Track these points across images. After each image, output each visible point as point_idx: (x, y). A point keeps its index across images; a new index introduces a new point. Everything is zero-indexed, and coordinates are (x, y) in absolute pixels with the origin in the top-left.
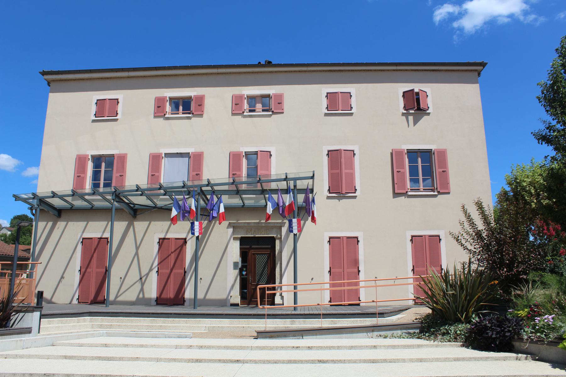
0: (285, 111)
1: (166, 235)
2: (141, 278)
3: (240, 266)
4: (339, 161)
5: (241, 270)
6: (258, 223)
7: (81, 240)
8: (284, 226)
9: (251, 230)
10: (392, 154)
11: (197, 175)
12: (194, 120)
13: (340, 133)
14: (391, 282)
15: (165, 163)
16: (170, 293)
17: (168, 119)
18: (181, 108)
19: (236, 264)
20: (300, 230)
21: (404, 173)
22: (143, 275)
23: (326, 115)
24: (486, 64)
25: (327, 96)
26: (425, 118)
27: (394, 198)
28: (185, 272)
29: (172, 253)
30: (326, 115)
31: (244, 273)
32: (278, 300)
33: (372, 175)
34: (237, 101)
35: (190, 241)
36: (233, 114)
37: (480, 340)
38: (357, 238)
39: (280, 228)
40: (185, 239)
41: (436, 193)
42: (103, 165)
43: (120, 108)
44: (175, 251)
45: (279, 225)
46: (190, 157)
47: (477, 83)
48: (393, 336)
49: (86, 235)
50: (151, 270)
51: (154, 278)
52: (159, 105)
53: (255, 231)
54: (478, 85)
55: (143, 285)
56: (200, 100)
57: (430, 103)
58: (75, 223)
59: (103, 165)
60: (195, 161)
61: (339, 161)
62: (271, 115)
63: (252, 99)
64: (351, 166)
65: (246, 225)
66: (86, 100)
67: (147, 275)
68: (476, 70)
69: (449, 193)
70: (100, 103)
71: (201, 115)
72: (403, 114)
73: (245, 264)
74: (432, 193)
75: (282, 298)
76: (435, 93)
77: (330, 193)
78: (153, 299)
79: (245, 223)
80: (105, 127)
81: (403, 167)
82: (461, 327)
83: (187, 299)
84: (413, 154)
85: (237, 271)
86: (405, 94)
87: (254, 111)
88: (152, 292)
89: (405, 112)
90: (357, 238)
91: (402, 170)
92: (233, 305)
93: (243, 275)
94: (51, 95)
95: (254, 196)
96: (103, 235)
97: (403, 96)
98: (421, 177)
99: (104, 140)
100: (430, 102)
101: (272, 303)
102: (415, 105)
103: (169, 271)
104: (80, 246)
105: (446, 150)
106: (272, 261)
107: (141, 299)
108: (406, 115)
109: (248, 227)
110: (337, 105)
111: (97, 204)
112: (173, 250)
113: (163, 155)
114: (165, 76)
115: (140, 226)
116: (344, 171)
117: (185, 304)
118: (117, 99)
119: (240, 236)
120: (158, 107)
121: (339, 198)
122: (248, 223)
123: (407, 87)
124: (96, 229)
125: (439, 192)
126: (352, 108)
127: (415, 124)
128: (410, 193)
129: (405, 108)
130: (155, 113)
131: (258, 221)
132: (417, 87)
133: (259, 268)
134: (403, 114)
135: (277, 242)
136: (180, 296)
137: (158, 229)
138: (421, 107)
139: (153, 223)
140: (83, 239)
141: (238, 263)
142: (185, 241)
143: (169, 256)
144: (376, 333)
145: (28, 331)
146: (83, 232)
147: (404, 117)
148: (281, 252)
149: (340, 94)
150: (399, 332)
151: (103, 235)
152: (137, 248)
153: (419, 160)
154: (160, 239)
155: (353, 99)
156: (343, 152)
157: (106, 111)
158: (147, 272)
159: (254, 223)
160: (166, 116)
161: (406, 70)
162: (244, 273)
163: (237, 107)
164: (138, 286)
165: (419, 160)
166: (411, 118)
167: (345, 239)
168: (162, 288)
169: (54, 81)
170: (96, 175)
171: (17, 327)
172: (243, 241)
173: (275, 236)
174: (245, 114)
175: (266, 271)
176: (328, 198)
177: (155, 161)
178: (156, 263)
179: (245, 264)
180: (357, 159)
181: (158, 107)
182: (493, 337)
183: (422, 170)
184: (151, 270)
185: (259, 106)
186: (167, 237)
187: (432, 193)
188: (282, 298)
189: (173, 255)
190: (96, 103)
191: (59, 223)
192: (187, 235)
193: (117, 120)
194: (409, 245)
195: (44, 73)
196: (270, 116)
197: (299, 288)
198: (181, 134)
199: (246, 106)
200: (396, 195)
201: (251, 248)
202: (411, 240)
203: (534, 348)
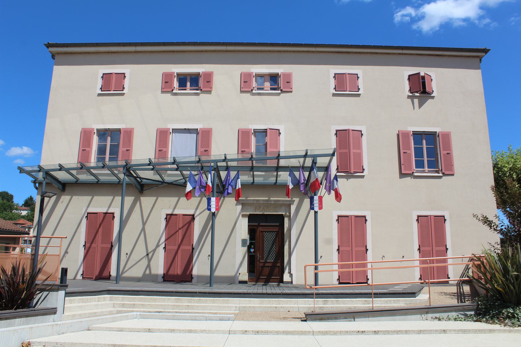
0: (293, 90)
2: (148, 255)
3: (248, 243)
5: (249, 248)
6: (267, 200)
7: (86, 215)
8: (293, 204)
9: (260, 207)
11: (205, 151)
12: (203, 96)
15: (173, 138)
16: (178, 270)
17: (176, 94)
18: (188, 84)
19: (244, 242)
20: (321, 208)
21: (410, 154)
22: (149, 251)
24: (489, 50)
25: (334, 77)
26: (430, 101)
27: (400, 178)
28: (193, 249)
29: (180, 229)
30: (334, 95)
31: (252, 250)
32: (286, 277)
33: (379, 155)
35: (198, 217)
36: (242, 92)
38: (365, 217)
39: (289, 206)
40: (193, 215)
41: (441, 175)
44: (182, 227)
45: (288, 203)
49: (91, 210)
50: (158, 246)
51: (161, 253)
52: (167, 79)
53: (263, 209)
54: (480, 70)
55: (149, 261)
56: (209, 77)
57: (434, 86)
58: (80, 197)
60: (203, 137)
62: (279, 94)
64: (359, 146)
65: (255, 202)
66: (93, 73)
67: (154, 251)
68: (478, 57)
69: (453, 175)
70: (106, 77)
71: (209, 92)
72: (409, 97)
73: (254, 241)
74: (437, 174)
75: (291, 275)
76: (439, 77)
78: (160, 275)
79: (254, 200)
80: (111, 102)
81: (409, 149)
83: (195, 276)
84: (418, 136)
85: (246, 248)
89: (411, 94)
90: (365, 217)
91: (408, 151)
92: (241, 282)
93: (250, 252)
94: (55, 67)
95: (263, 173)
96: (108, 210)
97: (409, 79)
98: (426, 159)
99: (110, 114)
100: (434, 85)
101: (281, 281)
102: (420, 88)
104: (84, 221)
105: (450, 132)
106: (280, 238)
107: (147, 275)
109: (257, 204)
110: (344, 86)
111: (102, 178)
112: (180, 226)
113: (171, 131)
115: (147, 201)
116: (352, 151)
117: (193, 280)
118: (124, 74)
119: (248, 213)
122: (257, 200)
123: (413, 70)
124: (101, 204)
125: (443, 173)
127: (420, 106)
128: (416, 174)
129: (411, 91)
130: (162, 88)
131: (267, 199)
132: (422, 71)
133: (267, 246)
134: (409, 97)
135: (286, 220)
136: (188, 273)
138: (427, 90)
139: (160, 199)
140: (88, 213)
141: (246, 240)
142: (193, 217)
143: (176, 232)
144: (430, 315)
145: (53, 311)
146: (88, 207)
147: (410, 100)
148: (290, 230)
149: (347, 76)
150: (454, 314)
151: (108, 210)
152: (144, 224)
153: (424, 141)
154: (167, 215)
156: (351, 132)
157: (112, 85)
158: (154, 248)
159: (264, 200)
160: (174, 91)
161: (411, 54)
162: (252, 250)
163: (246, 85)
164: (145, 262)
165: (424, 141)
166: (416, 101)
167: (353, 218)
168: (170, 264)
171: (39, 307)
172: (251, 218)
173: (284, 213)
174: (254, 91)
175: (274, 249)
177: (163, 136)
178: (163, 239)
179: (254, 241)
180: (364, 139)
183: (427, 153)
184: (158, 246)
186: (175, 213)
187: (437, 174)
188: (291, 275)
189: (180, 231)
190: (102, 77)
191: (63, 197)
192: (195, 212)
193: (123, 94)
194: (415, 224)
195: (49, 46)
196: (279, 94)
198: (188, 110)
200: (402, 175)
201: (259, 226)
202: (417, 220)
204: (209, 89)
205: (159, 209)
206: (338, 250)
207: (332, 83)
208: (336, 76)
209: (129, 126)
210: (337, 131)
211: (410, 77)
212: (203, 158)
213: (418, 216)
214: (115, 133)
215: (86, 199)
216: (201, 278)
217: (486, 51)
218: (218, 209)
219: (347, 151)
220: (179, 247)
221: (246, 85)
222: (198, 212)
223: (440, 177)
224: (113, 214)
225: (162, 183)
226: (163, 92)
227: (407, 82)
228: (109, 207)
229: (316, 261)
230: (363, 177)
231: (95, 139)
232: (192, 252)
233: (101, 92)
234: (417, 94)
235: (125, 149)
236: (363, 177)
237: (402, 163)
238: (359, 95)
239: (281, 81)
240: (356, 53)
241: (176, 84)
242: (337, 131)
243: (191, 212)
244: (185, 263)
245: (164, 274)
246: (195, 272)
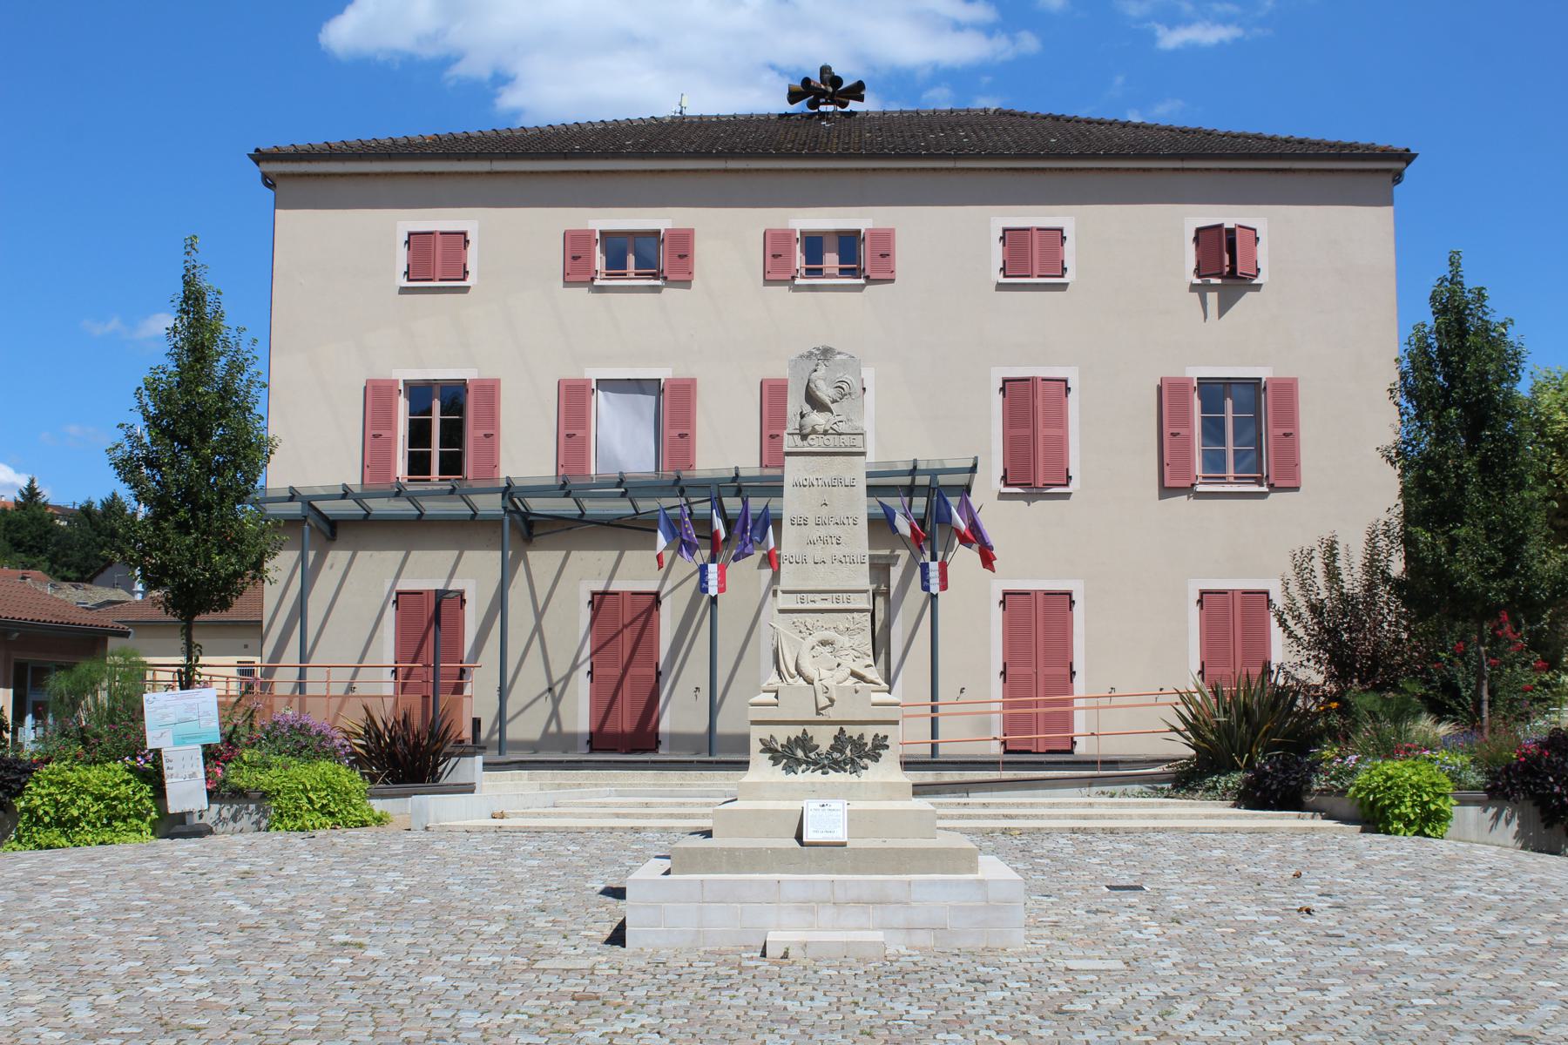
0: (898, 275)
1: (609, 584)
2: (550, 690)
4: (1030, 408)
7: (394, 597)
10: (1160, 389)
11: (681, 436)
12: (670, 293)
14: (1152, 699)
16: (625, 721)
17: (601, 289)
18: (631, 259)
20: (944, 587)
21: (1188, 440)
22: (555, 679)
23: (1001, 287)
26: (1249, 295)
28: (659, 674)
29: (625, 626)
30: (1001, 287)
33: (1108, 440)
34: (776, 247)
36: (767, 282)
37: (1256, 797)
38: (1069, 594)
40: (657, 594)
41: (1265, 489)
42: (436, 405)
45: (884, 561)
47: (1387, 201)
48: (1124, 794)
49: (404, 585)
50: (575, 666)
51: (582, 686)
52: (576, 248)
55: (556, 702)
56: (682, 243)
58: (376, 554)
59: (436, 405)
61: (1030, 408)
62: (863, 286)
63: (814, 244)
64: (1061, 421)
66: (382, 231)
68: (1388, 171)
69: (1296, 489)
70: (416, 241)
71: (686, 284)
72: (1193, 288)
74: (1256, 488)
76: (1278, 230)
77: (1006, 485)
78: (583, 734)
81: (1188, 423)
82: (1237, 778)
83: (665, 734)
84: (1213, 391)
87: (817, 272)
88: (579, 717)
89: (1199, 281)
90: (1069, 594)
91: (1183, 431)
97: (1196, 239)
102: (1223, 264)
103: (619, 671)
104: (391, 611)
105: (1295, 380)
107: (552, 735)
108: (1200, 290)
110: (1030, 261)
111: (432, 507)
113: (594, 386)
114: (588, 172)
115: (543, 561)
116: (1042, 432)
118: (464, 234)
120: (575, 258)
124: (427, 570)
125: (1271, 486)
126: (1064, 269)
127: (1221, 314)
128: (1200, 488)
129: (1199, 272)
134: (1193, 288)
136: (650, 728)
137: (587, 571)
138: (1239, 270)
140: (398, 593)
142: (656, 599)
143: (616, 635)
144: (1095, 789)
145: (468, 788)
146: (398, 577)
147: (1195, 296)
149: (1036, 234)
150: (1137, 788)
152: (539, 615)
153: (1229, 403)
154: (594, 594)
155: (1069, 246)
156: (1040, 383)
157: (435, 264)
160: (597, 282)
163: (775, 270)
164: (545, 706)
165: (1229, 403)
166: (1212, 297)
167: (1040, 598)
168: (605, 706)
169: (283, 175)
170: (419, 433)
174: (798, 281)
176: (1002, 496)
177: (574, 400)
178: (587, 651)
180: (1073, 400)
181: (575, 258)
183: (1233, 432)
184: (575, 666)
185: (831, 260)
186: (611, 589)
187: (1256, 488)
189: (627, 632)
190: (408, 242)
191: (332, 554)
192: (662, 585)
193: (466, 289)
194: (1194, 613)
195: (259, 157)
196: (860, 288)
197: (941, 709)
198: (633, 330)
199: (799, 260)
200: (1166, 491)
202: (1200, 601)
203: (1326, 802)
204: (685, 277)
205: (573, 579)
206: (1003, 673)
207: (997, 254)
209: (487, 374)
210: (1005, 381)
212: (684, 473)
213: (1203, 593)
214: (454, 396)
215: (393, 557)
216: (679, 740)
217: (1407, 157)
218: (722, 590)
219: (1028, 432)
221: (775, 270)
223: (1262, 495)
224: (461, 594)
226: (567, 284)
228: (451, 576)
229: (934, 697)
230: (1067, 496)
231: (402, 406)
232: (657, 681)
233: (406, 284)
234: (1214, 281)
235: (481, 433)
236: (1067, 496)
237: (1166, 460)
238: (1064, 287)
239: (866, 253)
240: (1061, 169)
241: (599, 261)
242: (1005, 381)
244: (642, 707)
245: (591, 734)
246: (665, 726)
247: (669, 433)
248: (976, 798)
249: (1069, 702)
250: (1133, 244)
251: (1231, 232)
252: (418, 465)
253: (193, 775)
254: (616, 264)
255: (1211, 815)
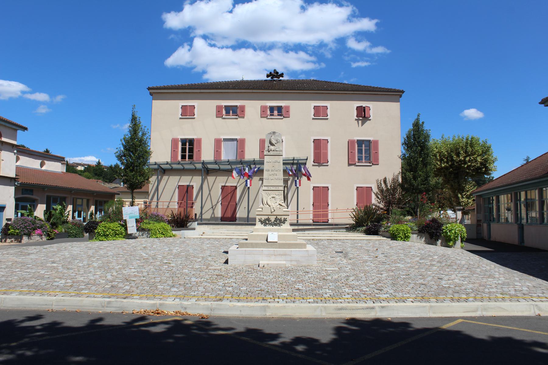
4: (320, 146)
13: (321, 129)
16: (229, 215)
18: (231, 112)
20: (300, 185)
21: (355, 153)
23: (313, 119)
24: (403, 92)
26: (368, 122)
30: (313, 119)
33: (337, 153)
34: (263, 109)
36: (261, 117)
37: (368, 232)
42: (187, 144)
43: (196, 111)
46: (237, 141)
47: (399, 102)
49: (180, 184)
50: (218, 202)
51: (219, 207)
52: (219, 109)
55: (214, 210)
56: (243, 108)
59: (187, 144)
60: (241, 144)
61: (320, 146)
63: (272, 109)
66: (176, 105)
67: (216, 205)
70: (183, 107)
71: (243, 117)
72: (356, 120)
76: (375, 108)
81: (354, 150)
82: (364, 228)
84: (360, 143)
86: (358, 108)
87: (273, 115)
88: (219, 213)
94: (154, 102)
98: (364, 155)
99: (187, 130)
100: (371, 112)
102: (363, 115)
104: (177, 190)
111: (187, 167)
115: (211, 179)
116: (322, 151)
121: (319, 166)
124: (185, 181)
127: (362, 125)
129: (357, 116)
132: (364, 104)
134: (356, 120)
137: (221, 181)
142: (236, 187)
145: (194, 229)
152: (210, 191)
153: (363, 145)
155: (329, 110)
157: (188, 113)
163: (263, 114)
164: (211, 211)
166: (360, 122)
168: (224, 211)
169: (154, 93)
170: (184, 150)
176: (313, 165)
177: (218, 143)
178: (220, 199)
182: (372, 231)
183: (364, 152)
184: (218, 202)
185: (276, 112)
191: (164, 177)
193: (194, 118)
195: (149, 89)
196: (282, 119)
198: (231, 128)
199: (269, 112)
200: (349, 165)
205: (217, 183)
208: (315, 107)
209: (199, 137)
211: (358, 108)
214: (191, 142)
215: (177, 178)
216: (241, 219)
217: (403, 92)
218: (251, 185)
220: (229, 203)
221: (263, 114)
222: (239, 185)
223: (371, 166)
224: (193, 186)
225: (219, 170)
226: (217, 117)
227: (355, 111)
229: (298, 210)
230: (327, 165)
231: (180, 144)
236: (327, 165)
238: (327, 119)
239: (283, 111)
243: (235, 185)
246: (238, 216)
247: (239, 150)
248: (307, 232)
249: (327, 211)
250: (342, 110)
251: (364, 107)
252: (183, 157)
253: (133, 226)
254: (228, 113)
255: (359, 236)
